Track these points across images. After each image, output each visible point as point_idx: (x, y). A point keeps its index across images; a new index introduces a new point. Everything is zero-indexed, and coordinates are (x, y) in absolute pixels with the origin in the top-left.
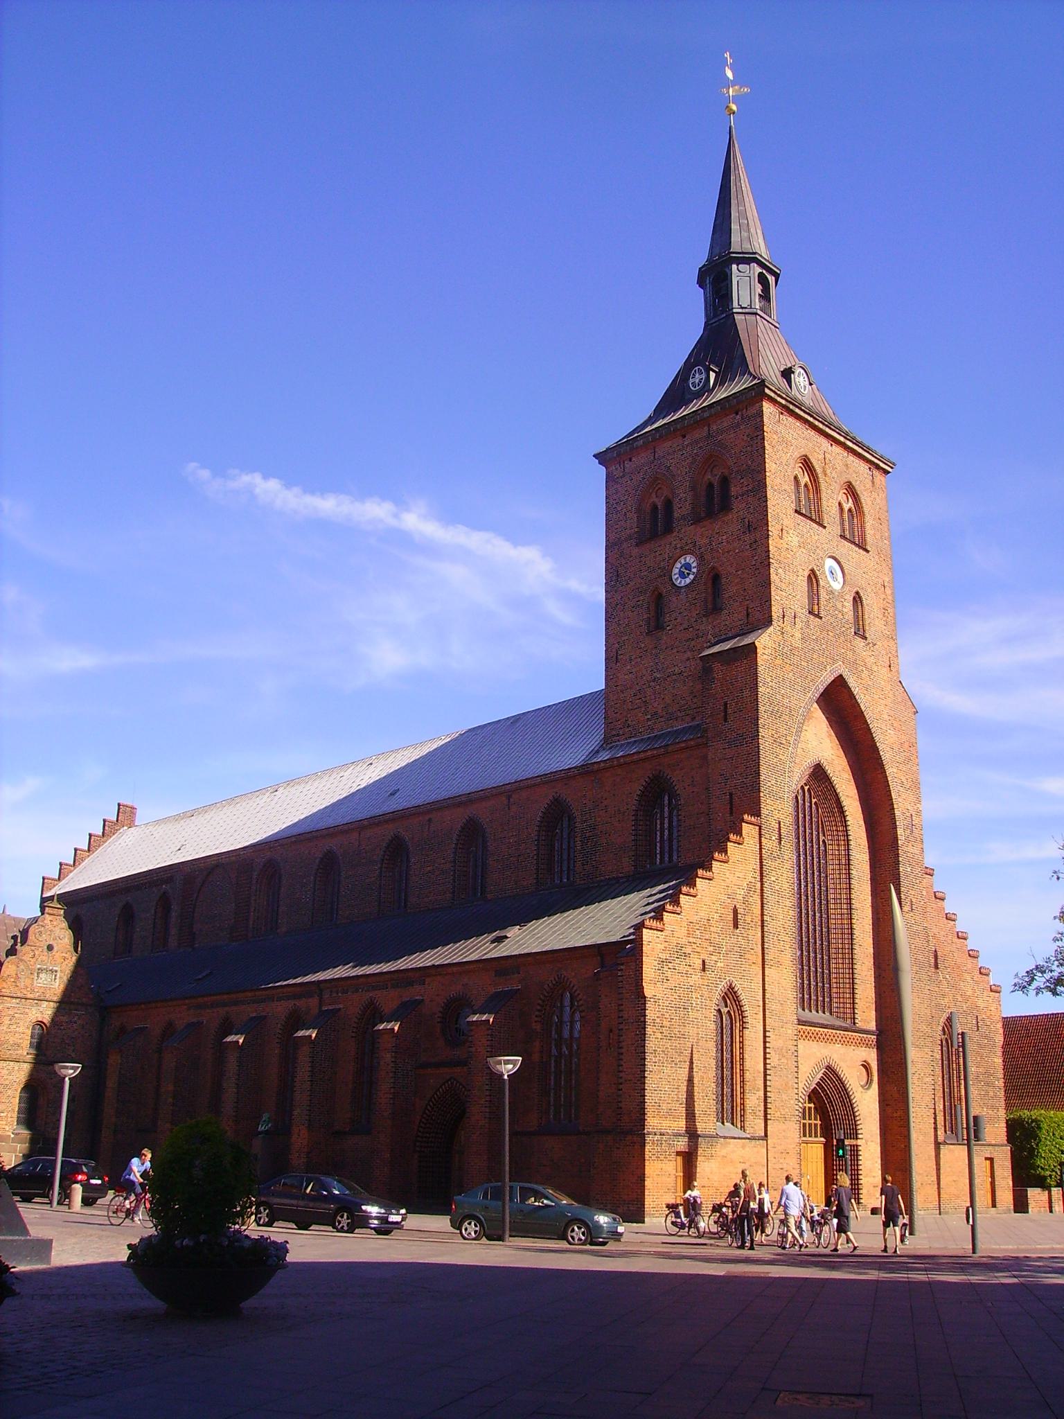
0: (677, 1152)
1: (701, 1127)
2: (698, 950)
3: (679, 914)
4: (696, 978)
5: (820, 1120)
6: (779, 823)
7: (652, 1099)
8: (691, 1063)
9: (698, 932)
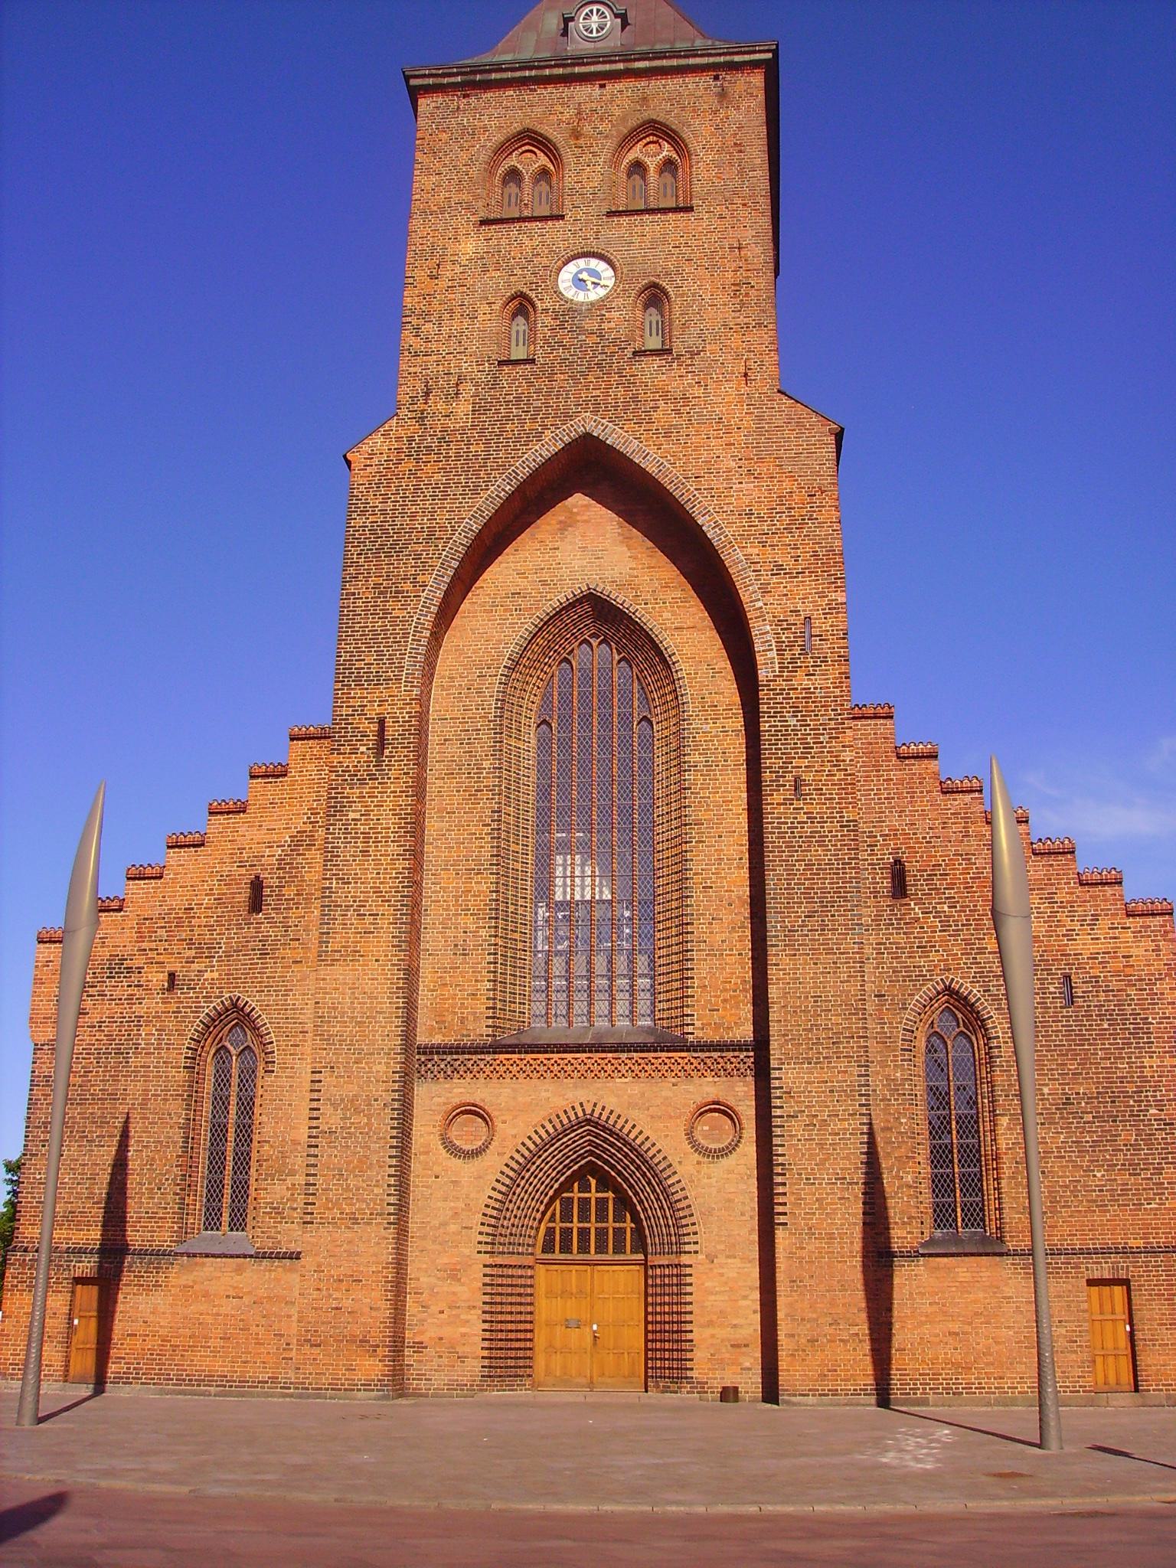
0: (74, 1278)
1: (135, 1237)
2: (161, 958)
3: (120, 910)
4: (152, 1004)
5: (632, 1221)
6: (382, 722)
7: (35, 1198)
8: (125, 1135)
9: (162, 933)
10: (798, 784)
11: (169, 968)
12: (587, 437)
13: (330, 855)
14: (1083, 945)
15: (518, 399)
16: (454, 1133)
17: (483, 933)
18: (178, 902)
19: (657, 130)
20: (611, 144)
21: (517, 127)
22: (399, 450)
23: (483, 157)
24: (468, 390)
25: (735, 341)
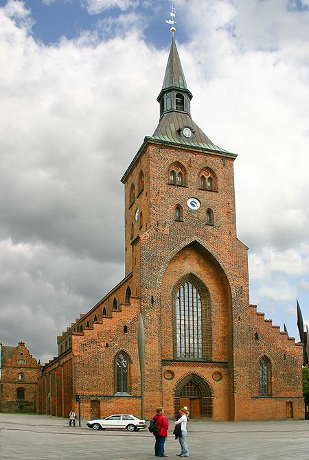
12: (195, 242)
14: (288, 350)
18: (107, 329)
19: (208, 169)
20: (198, 171)
21: (175, 160)
23: (167, 166)
24: (168, 225)
25: (227, 225)
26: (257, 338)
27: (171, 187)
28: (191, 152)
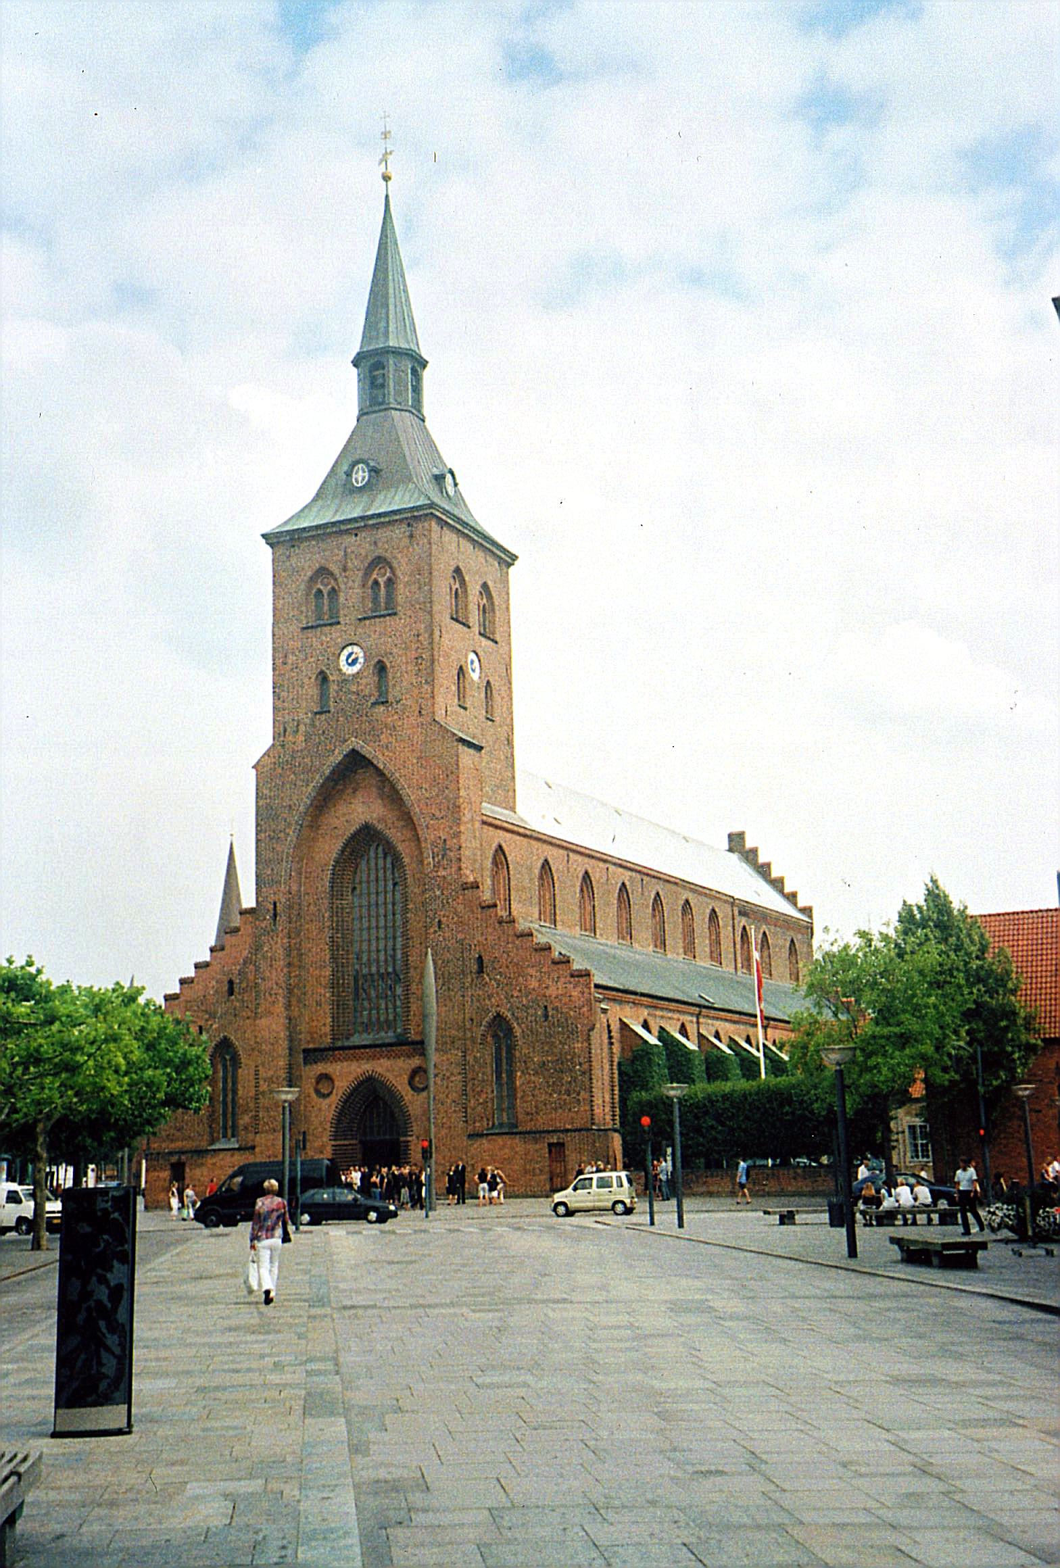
6: (275, 904)
10: (440, 922)
11: (199, 1024)
13: (257, 969)
14: (552, 991)
15: (324, 732)
16: (320, 1086)
17: (328, 995)
22: (275, 763)
24: (302, 728)
26: (481, 970)
27: (310, 633)
28: (347, 532)
